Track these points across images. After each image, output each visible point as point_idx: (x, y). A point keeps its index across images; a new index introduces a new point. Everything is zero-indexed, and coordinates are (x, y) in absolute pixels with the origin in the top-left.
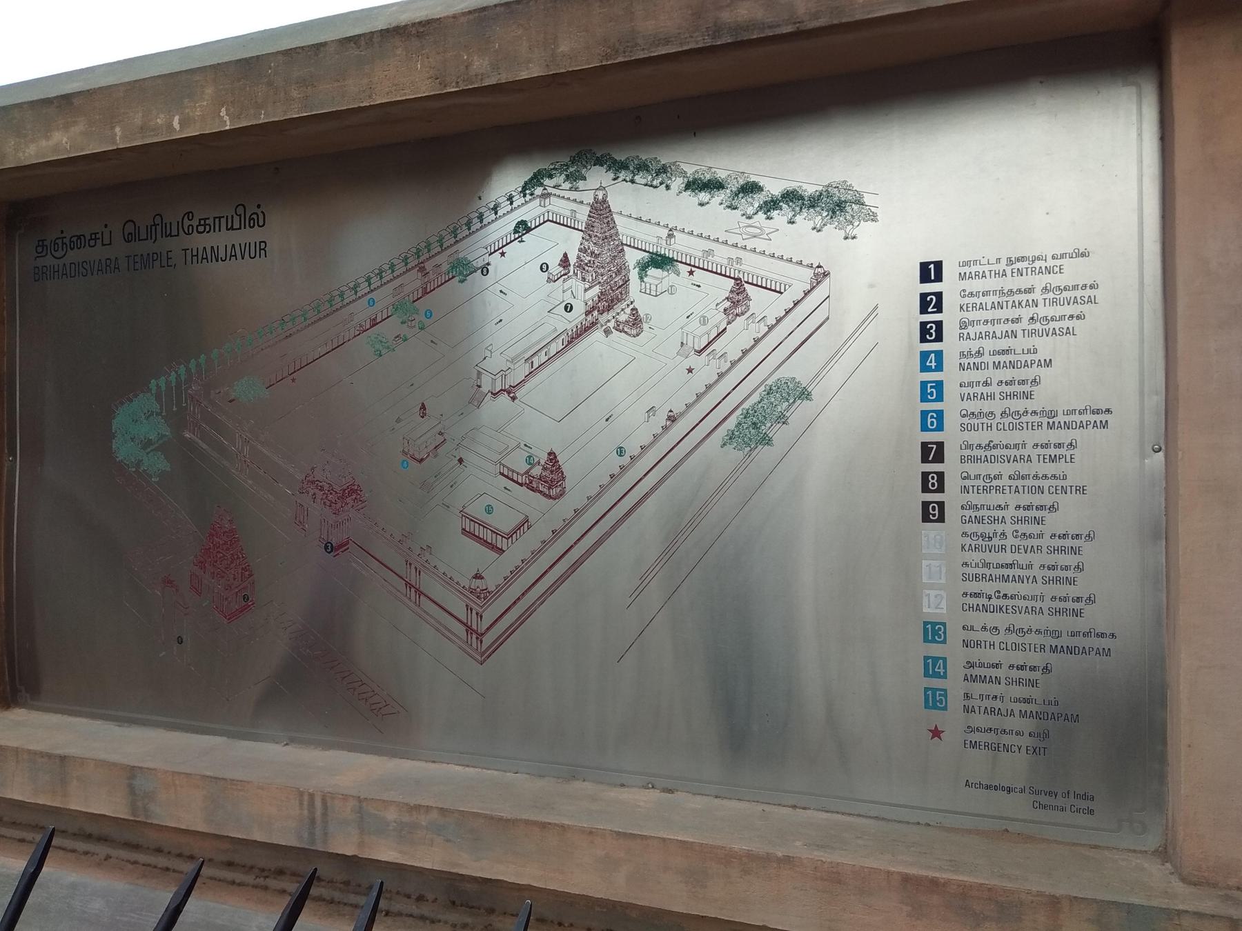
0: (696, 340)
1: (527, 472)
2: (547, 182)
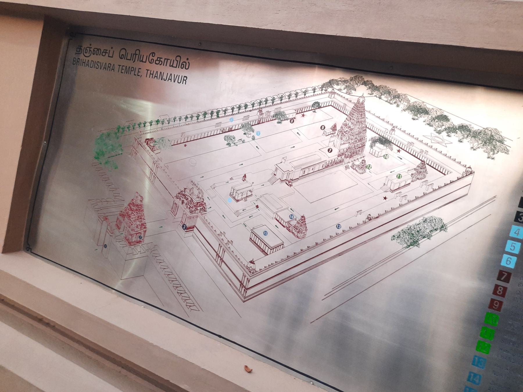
0: (393, 184)
1: (288, 222)
2: (335, 86)
